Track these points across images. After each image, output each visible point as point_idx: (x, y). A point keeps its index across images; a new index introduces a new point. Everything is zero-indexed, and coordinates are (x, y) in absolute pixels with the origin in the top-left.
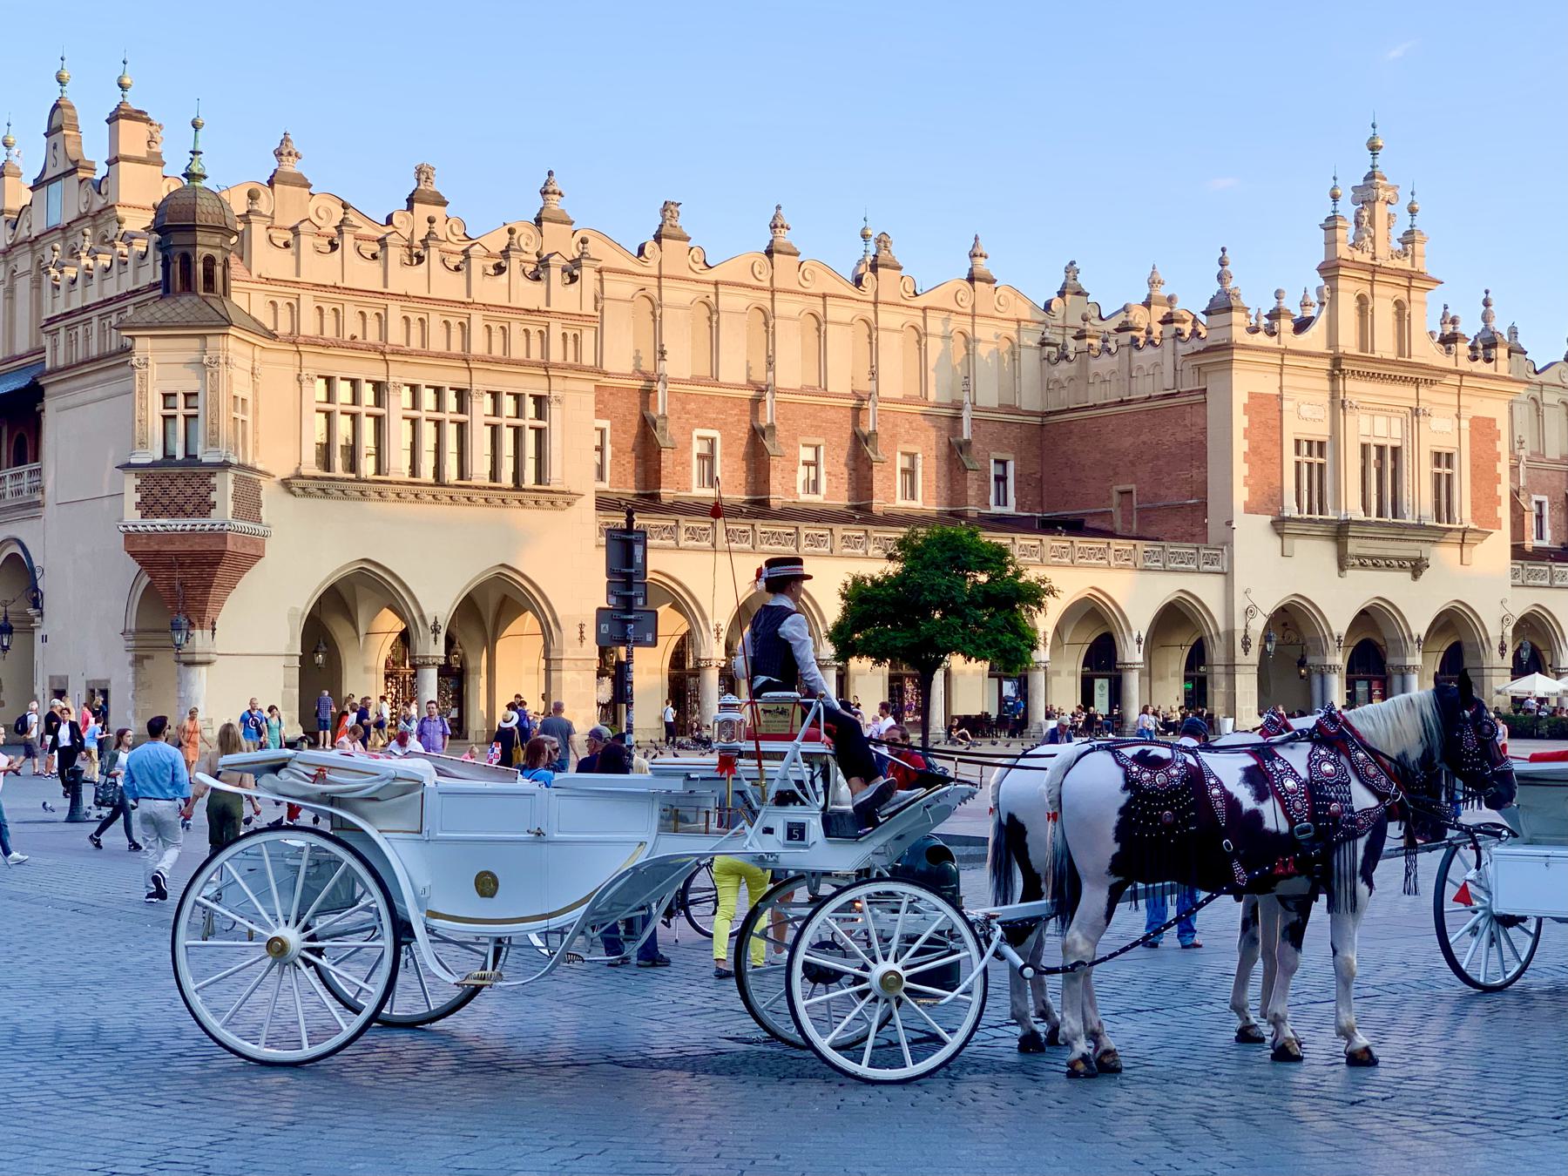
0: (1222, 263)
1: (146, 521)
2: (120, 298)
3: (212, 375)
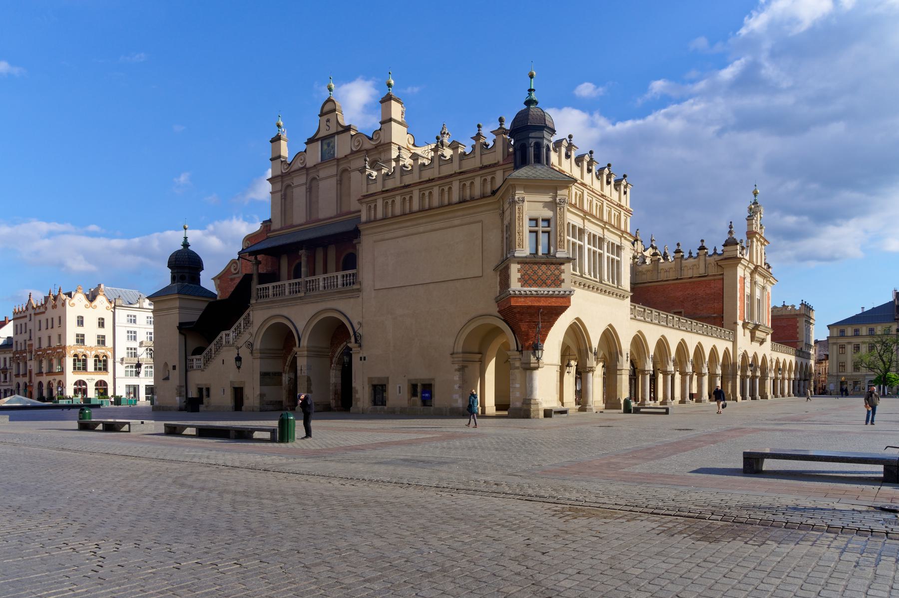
0: (731, 227)
1: (525, 289)
2: (451, 176)
3: (560, 209)
